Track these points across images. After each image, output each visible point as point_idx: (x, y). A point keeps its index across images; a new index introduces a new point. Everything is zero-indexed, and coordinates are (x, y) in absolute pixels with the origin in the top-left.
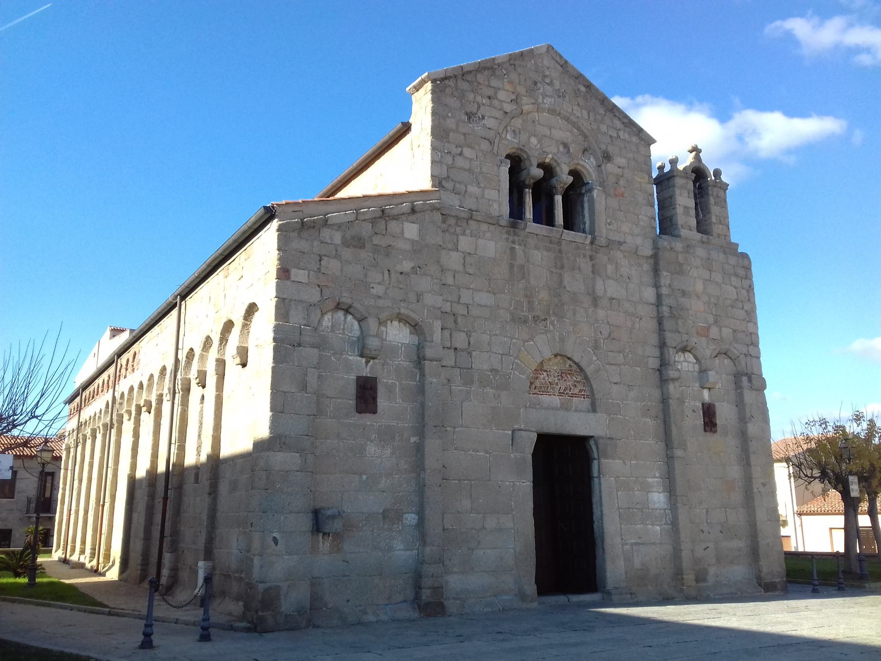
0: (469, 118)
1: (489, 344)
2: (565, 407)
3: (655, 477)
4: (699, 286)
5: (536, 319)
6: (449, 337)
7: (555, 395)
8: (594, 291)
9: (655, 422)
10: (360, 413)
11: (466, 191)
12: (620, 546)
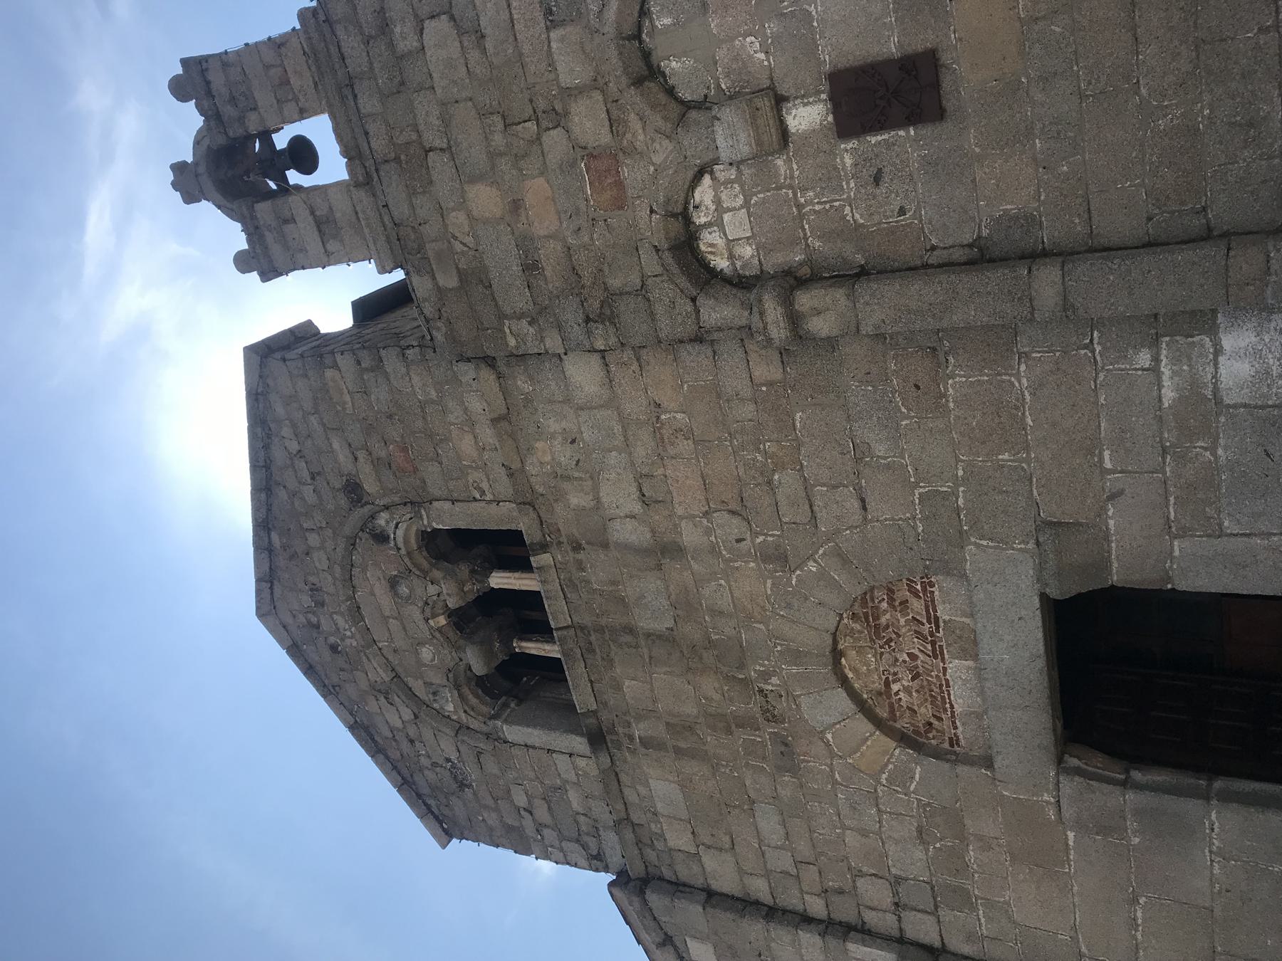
1: (864, 833)
2: (970, 648)
3: (1155, 370)
6: (874, 913)
7: (945, 669)
9: (951, 360)
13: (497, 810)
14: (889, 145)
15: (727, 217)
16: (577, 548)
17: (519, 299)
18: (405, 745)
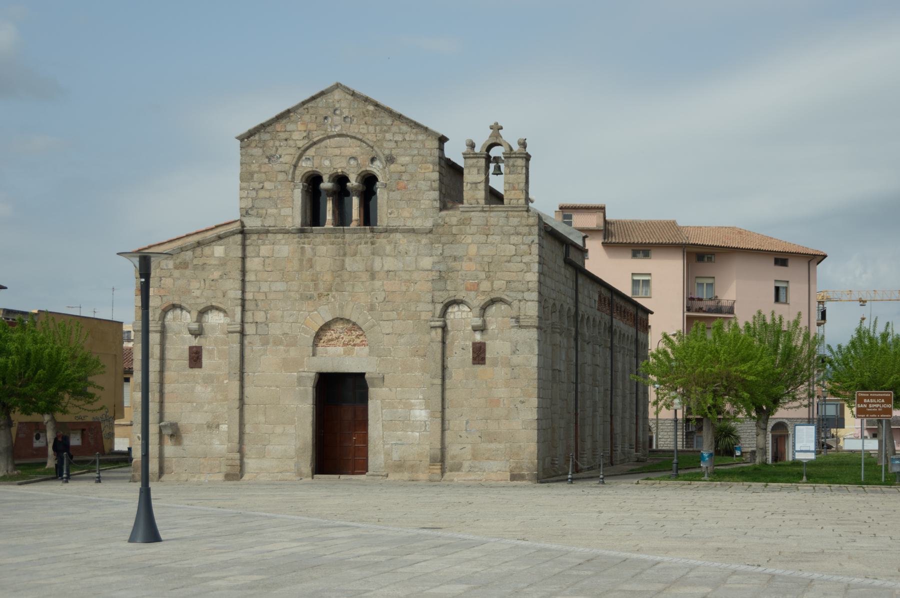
0: (269, 159)
1: (282, 317)
3: (418, 399)
4: (473, 250)
5: (320, 296)
8: (372, 268)
10: (192, 368)
11: (266, 213)
12: (382, 446)
13: (260, 172)
14: (469, 352)
15: (460, 313)
16: (372, 243)
17: (447, 253)
18: (283, 135)
